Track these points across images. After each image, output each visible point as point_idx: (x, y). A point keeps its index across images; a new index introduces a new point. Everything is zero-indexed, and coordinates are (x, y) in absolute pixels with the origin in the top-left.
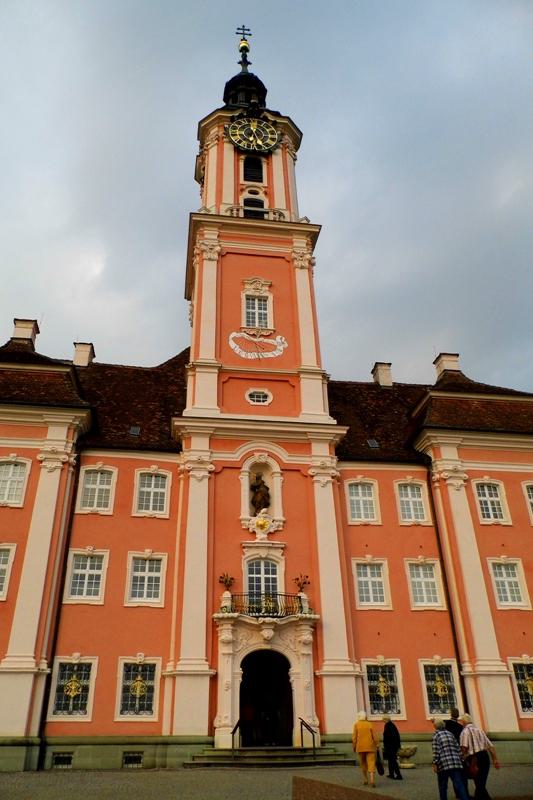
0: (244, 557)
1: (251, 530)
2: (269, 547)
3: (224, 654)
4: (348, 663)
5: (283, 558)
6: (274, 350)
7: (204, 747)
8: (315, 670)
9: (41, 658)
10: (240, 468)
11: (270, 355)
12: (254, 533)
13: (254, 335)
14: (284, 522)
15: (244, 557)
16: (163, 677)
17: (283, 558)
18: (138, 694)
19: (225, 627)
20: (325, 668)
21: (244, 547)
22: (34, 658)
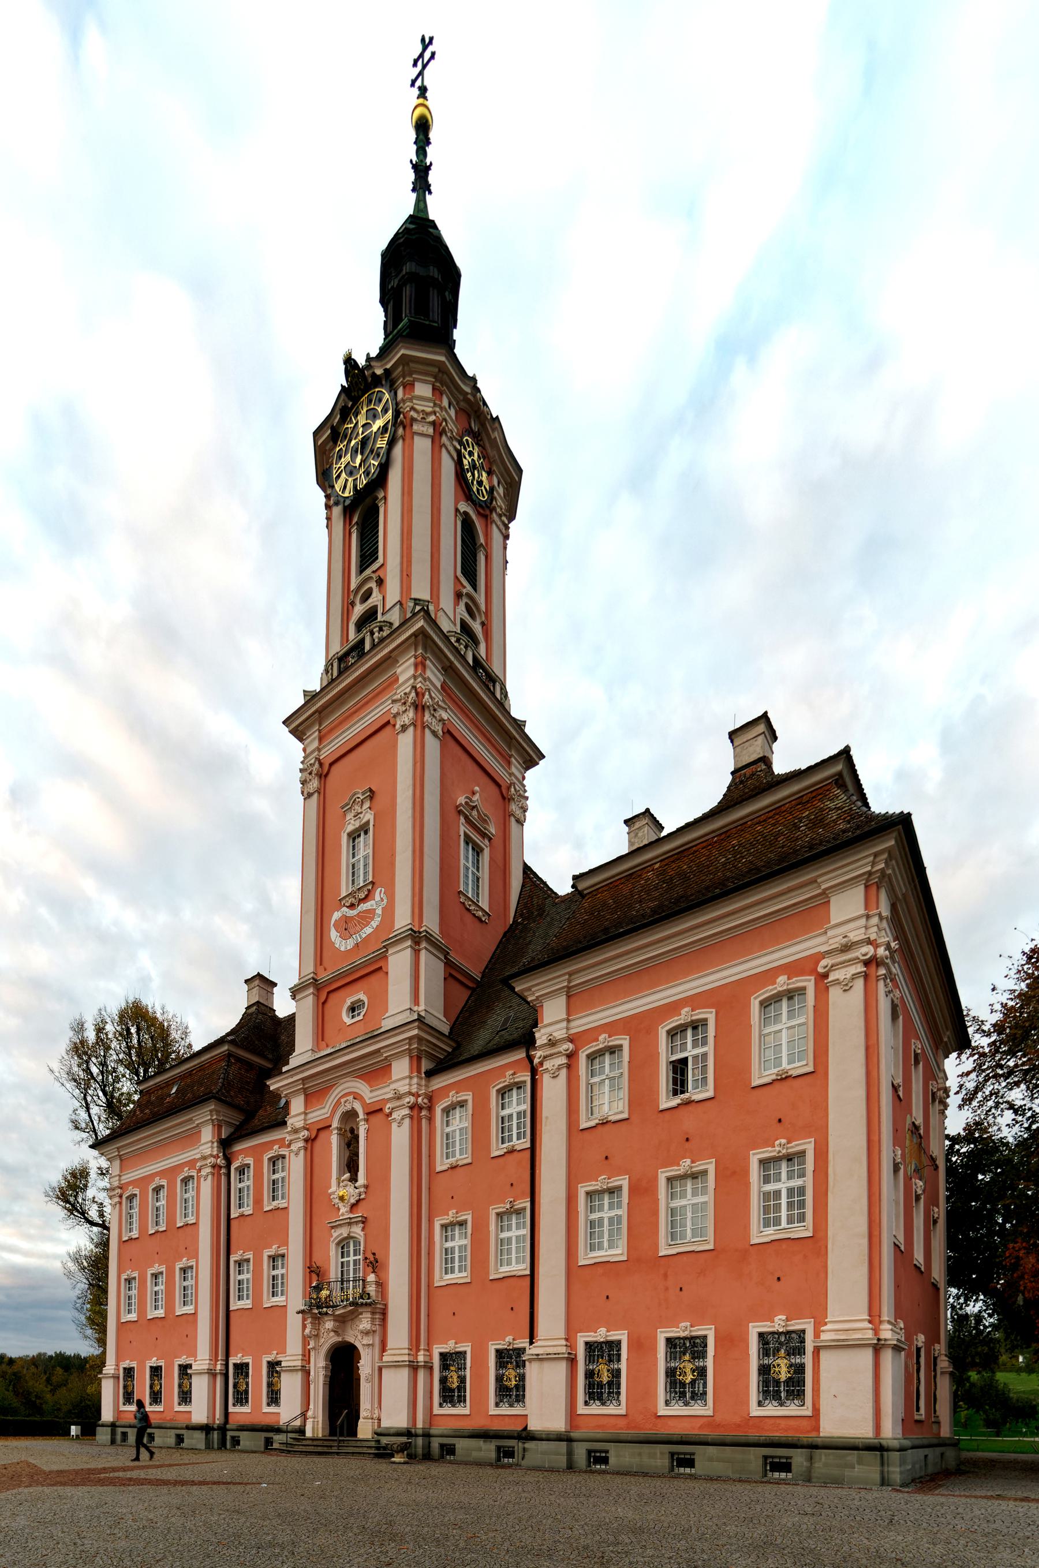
6: (372, 919)
9: (881, 1322)
10: (330, 1126)
11: (368, 930)
13: (352, 906)
16: (817, 1350)
18: (783, 1377)
22: (870, 1322)
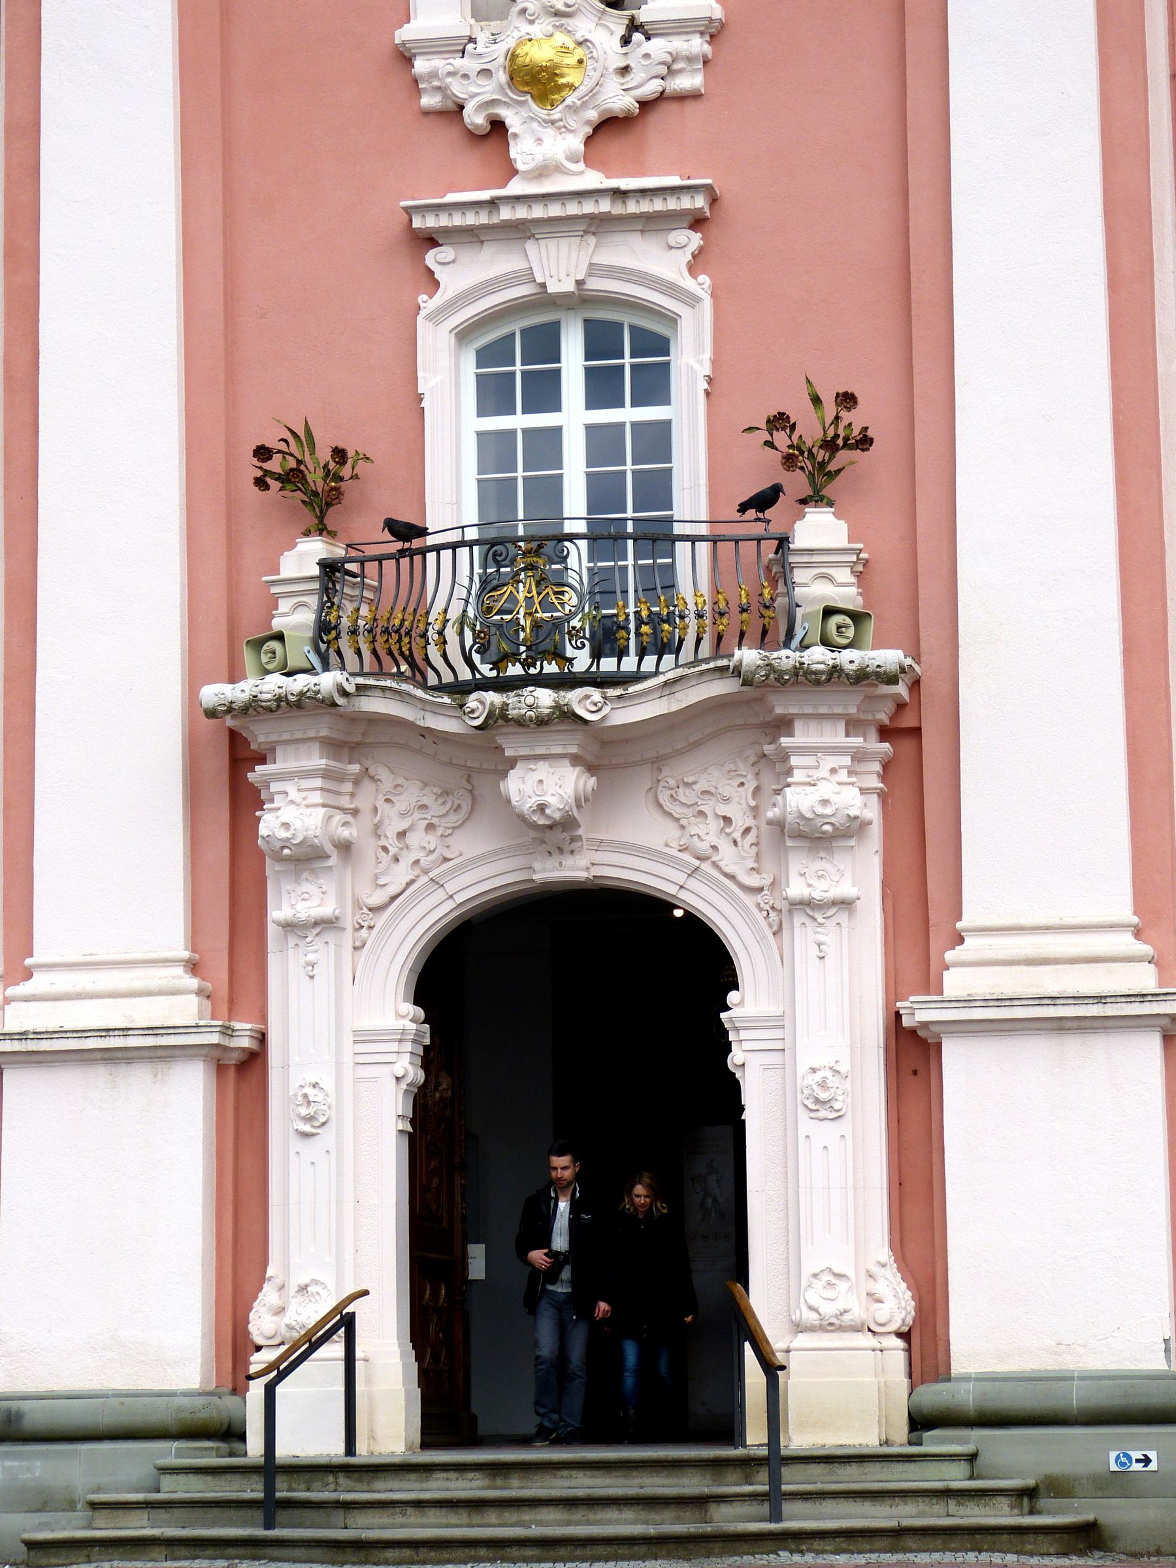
0: (429, 304)
1: (475, 118)
2: (597, 225)
3: (289, 926)
4: (1125, 943)
5: (700, 286)
7: (170, 1452)
8: (894, 988)
12: (498, 127)
14: (714, 32)
15: (429, 304)
17: (700, 286)
19: (283, 763)
20: (955, 983)
21: (431, 240)
